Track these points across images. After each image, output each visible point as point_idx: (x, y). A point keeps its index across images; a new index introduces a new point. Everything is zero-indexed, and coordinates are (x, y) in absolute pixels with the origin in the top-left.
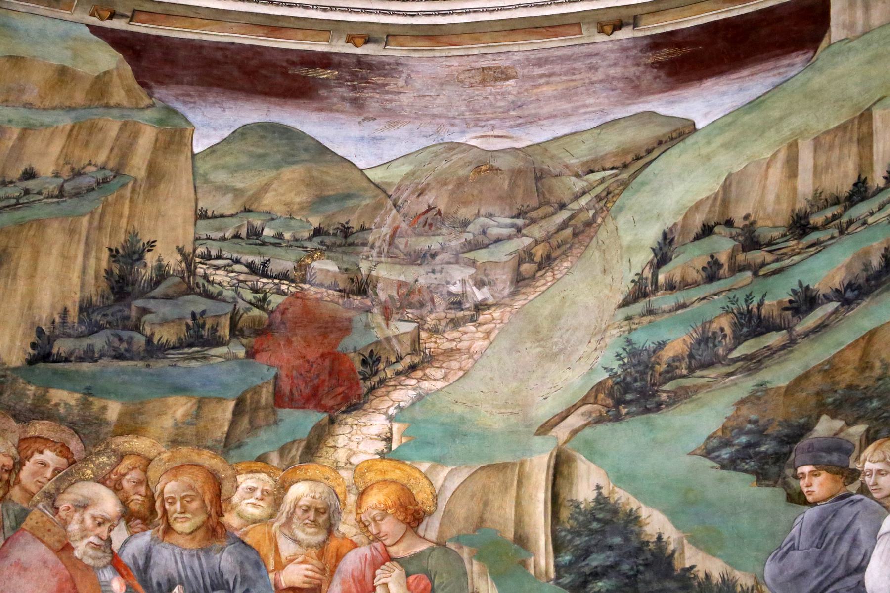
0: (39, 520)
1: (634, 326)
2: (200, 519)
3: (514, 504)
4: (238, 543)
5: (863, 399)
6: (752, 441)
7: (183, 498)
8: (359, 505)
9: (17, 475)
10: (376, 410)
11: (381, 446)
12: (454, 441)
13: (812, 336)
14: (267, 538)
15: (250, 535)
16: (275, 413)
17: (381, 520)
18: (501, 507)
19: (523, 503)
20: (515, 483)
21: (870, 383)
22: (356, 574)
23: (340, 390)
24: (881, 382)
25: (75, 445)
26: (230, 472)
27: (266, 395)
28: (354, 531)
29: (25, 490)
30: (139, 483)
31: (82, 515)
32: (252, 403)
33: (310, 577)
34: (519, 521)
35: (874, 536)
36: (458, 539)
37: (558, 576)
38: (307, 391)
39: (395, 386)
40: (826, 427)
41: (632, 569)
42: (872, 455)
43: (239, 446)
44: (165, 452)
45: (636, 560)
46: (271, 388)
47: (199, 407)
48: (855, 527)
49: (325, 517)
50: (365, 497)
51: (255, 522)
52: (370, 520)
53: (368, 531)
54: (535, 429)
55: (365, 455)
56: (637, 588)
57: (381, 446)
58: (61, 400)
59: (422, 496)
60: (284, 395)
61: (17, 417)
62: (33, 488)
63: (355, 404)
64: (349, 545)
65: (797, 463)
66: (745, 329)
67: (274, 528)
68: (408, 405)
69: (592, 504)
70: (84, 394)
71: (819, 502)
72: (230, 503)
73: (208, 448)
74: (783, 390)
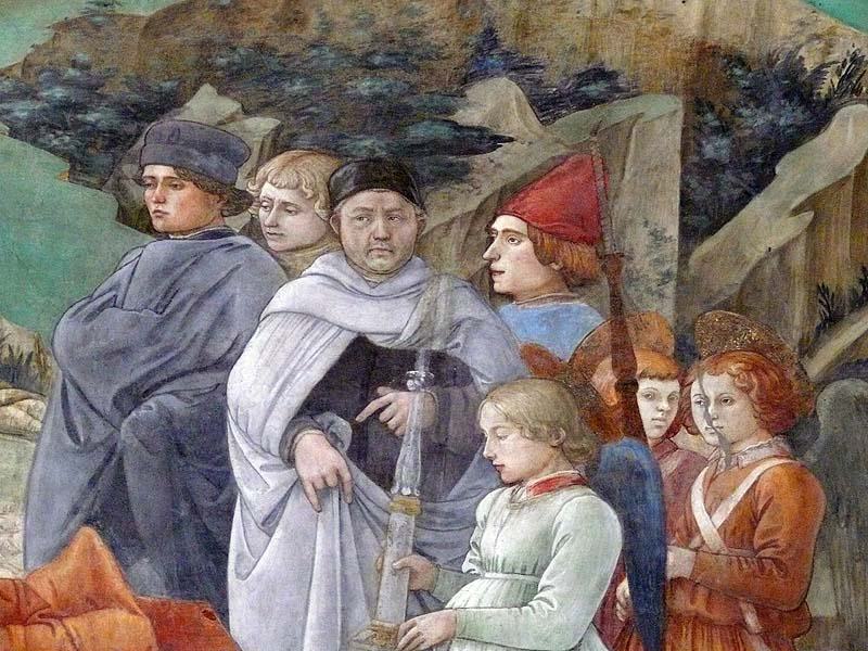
5: (279, 73)
21: (292, 48)
24: (315, 52)
35: (257, 315)
40: (206, 106)
42: (278, 174)
48: (227, 290)
65: (146, 157)
71: (172, 234)
74: (142, 24)
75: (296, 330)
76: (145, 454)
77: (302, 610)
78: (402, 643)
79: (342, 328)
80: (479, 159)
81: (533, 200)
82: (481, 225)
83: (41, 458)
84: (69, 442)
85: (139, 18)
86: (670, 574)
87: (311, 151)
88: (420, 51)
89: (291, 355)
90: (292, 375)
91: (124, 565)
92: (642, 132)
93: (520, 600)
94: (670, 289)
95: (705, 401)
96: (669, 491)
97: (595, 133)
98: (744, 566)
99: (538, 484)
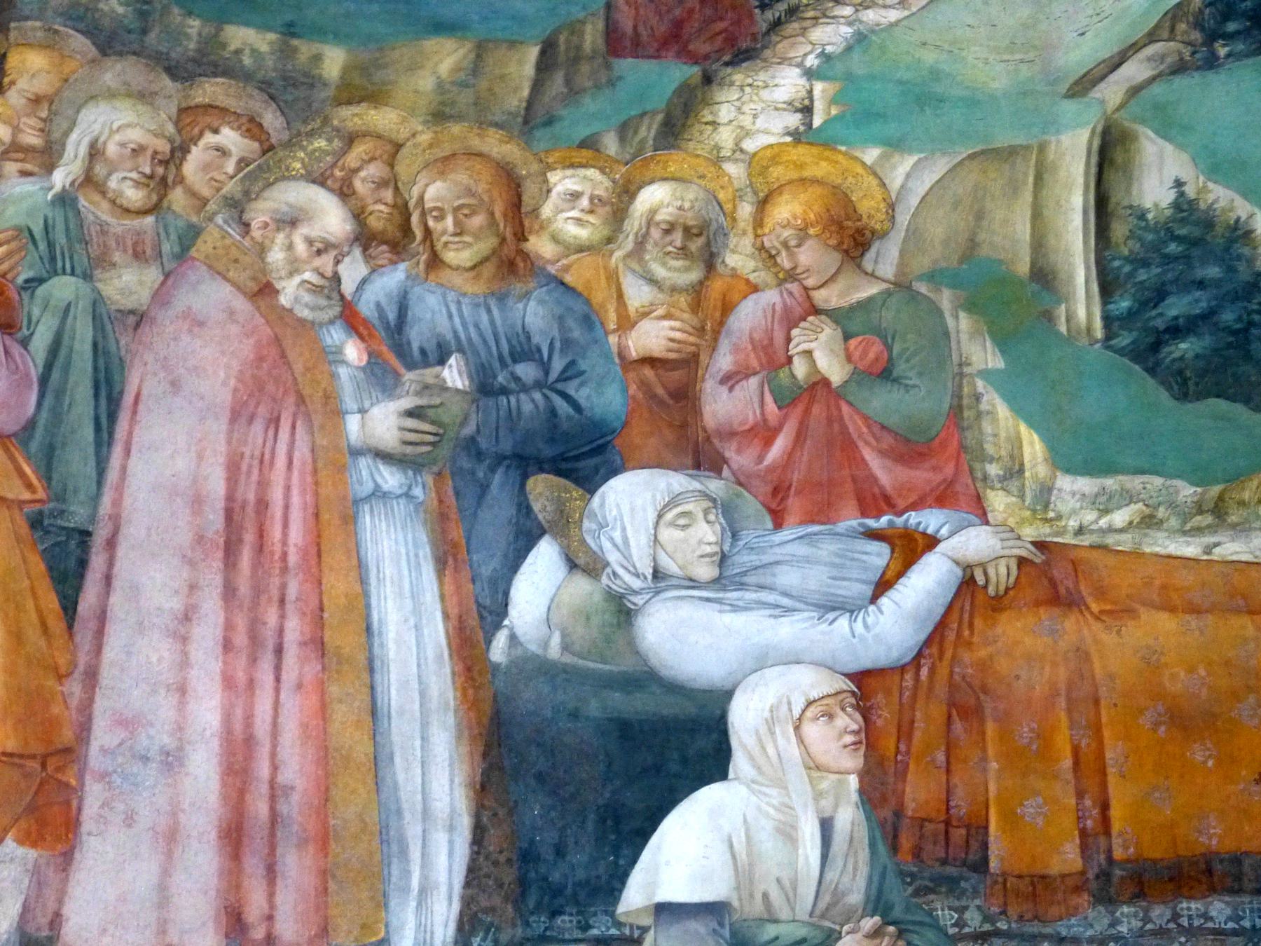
0: (218, 244)
2: (487, 244)
3: (1028, 214)
4: (553, 285)
7: (456, 210)
8: (758, 222)
9: (179, 167)
10: (784, 61)
11: (794, 120)
12: (922, 110)
14: (603, 277)
15: (572, 271)
16: (608, 66)
17: (799, 246)
18: (1005, 222)
19: (1046, 212)
20: (1031, 179)
22: (756, 336)
23: (721, 25)
25: (272, 120)
26: (535, 167)
27: (592, 36)
28: (751, 264)
29: (193, 194)
30: (382, 184)
31: (289, 236)
32: (568, 49)
33: (679, 342)
34: (1038, 244)
36: (932, 277)
37: (1109, 336)
38: (662, 28)
39: (815, 18)
41: (1240, 319)
43: (549, 122)
44: (423, 132)
45: (1246, 304)
46: (601, 25)
47: (478, 56)
49: (700, 241)
50: (768, 206)
51: (580, 249)
52: (779, 247)
53: (776, 264)
54: (1063, 88)
55: (766, 136)
56: (1249, 351)
57: (794, 120)
58: (244, 44)
59: (869, 205)
60: (624, 34)
61: (173, 72)
62: (206, 192)
63: (747, 51)
64: (743, 287)
67: (613, 260)
68: (840, 50)
69: (1168, 213)
70: (282, 33)
72: (537, 217)
73: (498, 125)
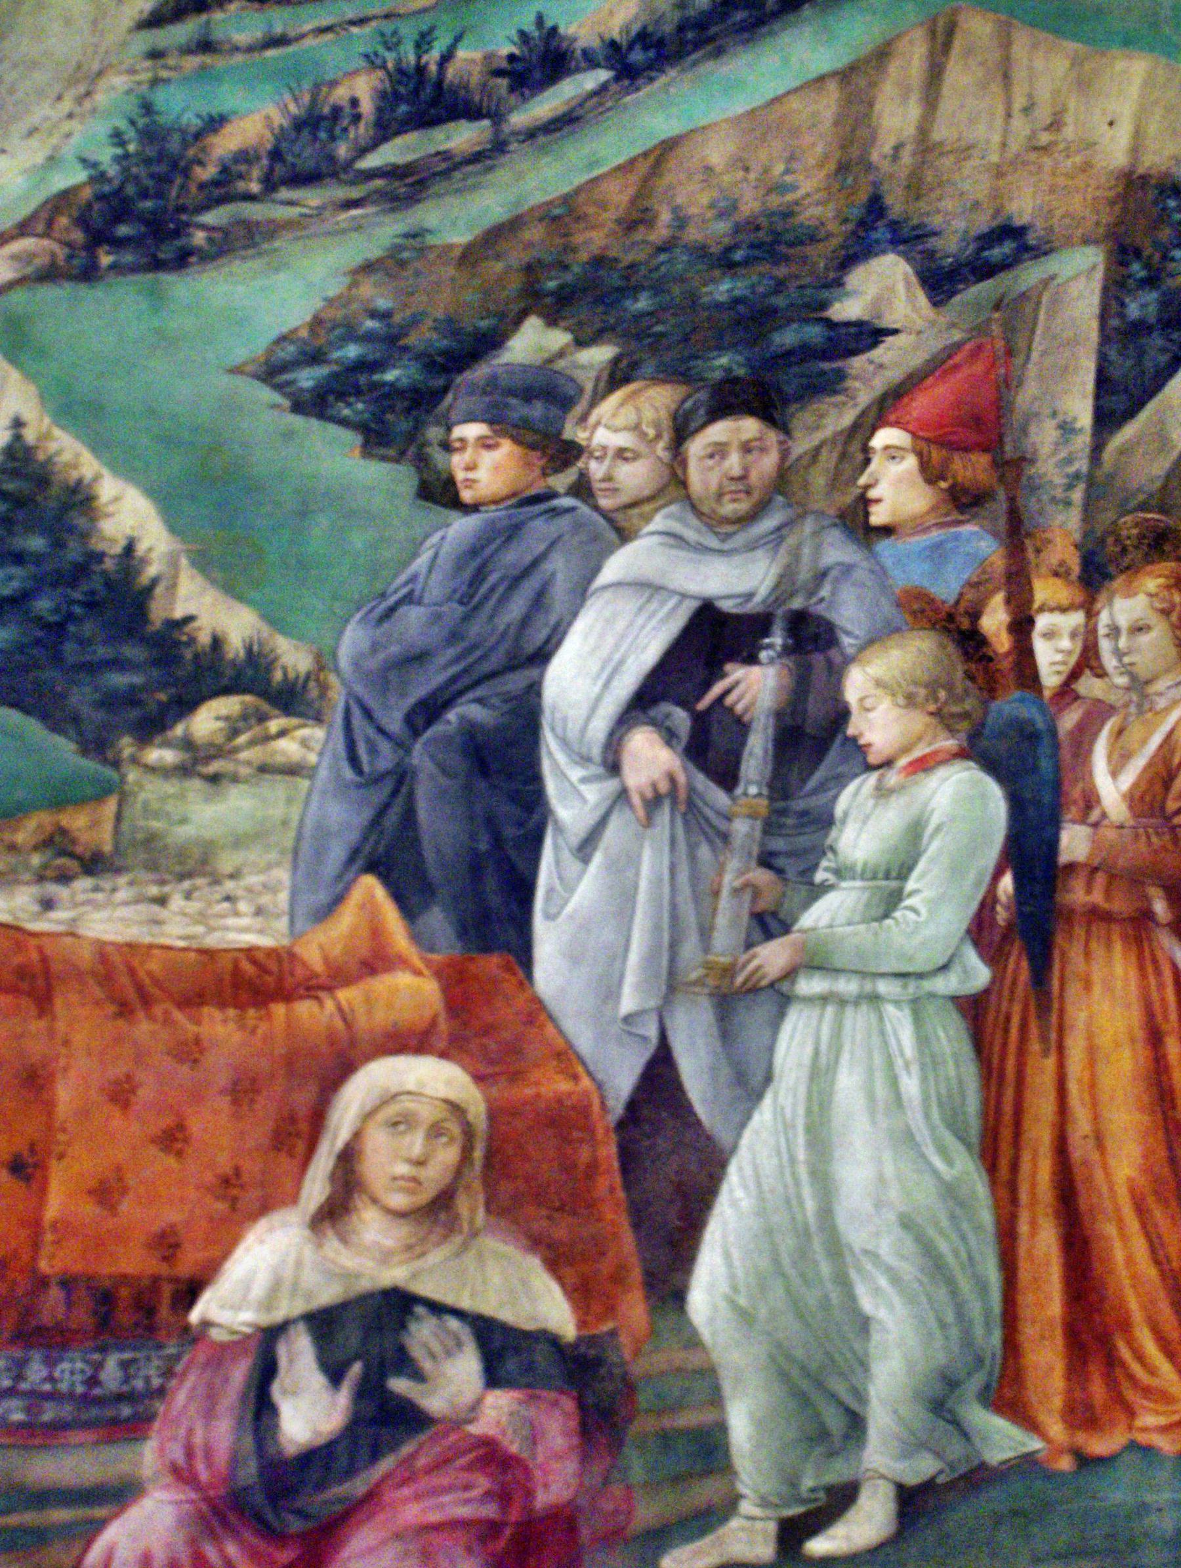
1: (164, 74)
5: (618, 289)
6: (371, 357)
13: (542, 139)
24: (663, 257)
35: (581, 592)
41: (56, 610)
42: (614, 416)
48: (547, 567)
65: (454, 416)
66: (403, 108)
74: (457, 252)
75: (627, 604)
76: (443, 781)
77: (621, 950)
78: (740, 979)
79: (684, 596)
80: (857, 363)
81: (921, 405)
82: (855, 446)
83: (315, 798)
84: (348, 774)
85: (450, 247)
86: (1064, 858)
87: (656, 380)
88: (788, 237)
89: (623, 637)
90: (621, 662)
91: (409, 912)
92: (1054, 301)
93: (881, 911)
94: (1077, 495)
95: (1115, 631)
96: (1066, 754)
97: (997, 307)
98: (1154, 839)
99: (911, 764)
